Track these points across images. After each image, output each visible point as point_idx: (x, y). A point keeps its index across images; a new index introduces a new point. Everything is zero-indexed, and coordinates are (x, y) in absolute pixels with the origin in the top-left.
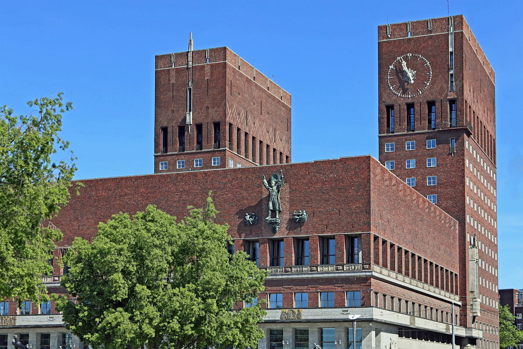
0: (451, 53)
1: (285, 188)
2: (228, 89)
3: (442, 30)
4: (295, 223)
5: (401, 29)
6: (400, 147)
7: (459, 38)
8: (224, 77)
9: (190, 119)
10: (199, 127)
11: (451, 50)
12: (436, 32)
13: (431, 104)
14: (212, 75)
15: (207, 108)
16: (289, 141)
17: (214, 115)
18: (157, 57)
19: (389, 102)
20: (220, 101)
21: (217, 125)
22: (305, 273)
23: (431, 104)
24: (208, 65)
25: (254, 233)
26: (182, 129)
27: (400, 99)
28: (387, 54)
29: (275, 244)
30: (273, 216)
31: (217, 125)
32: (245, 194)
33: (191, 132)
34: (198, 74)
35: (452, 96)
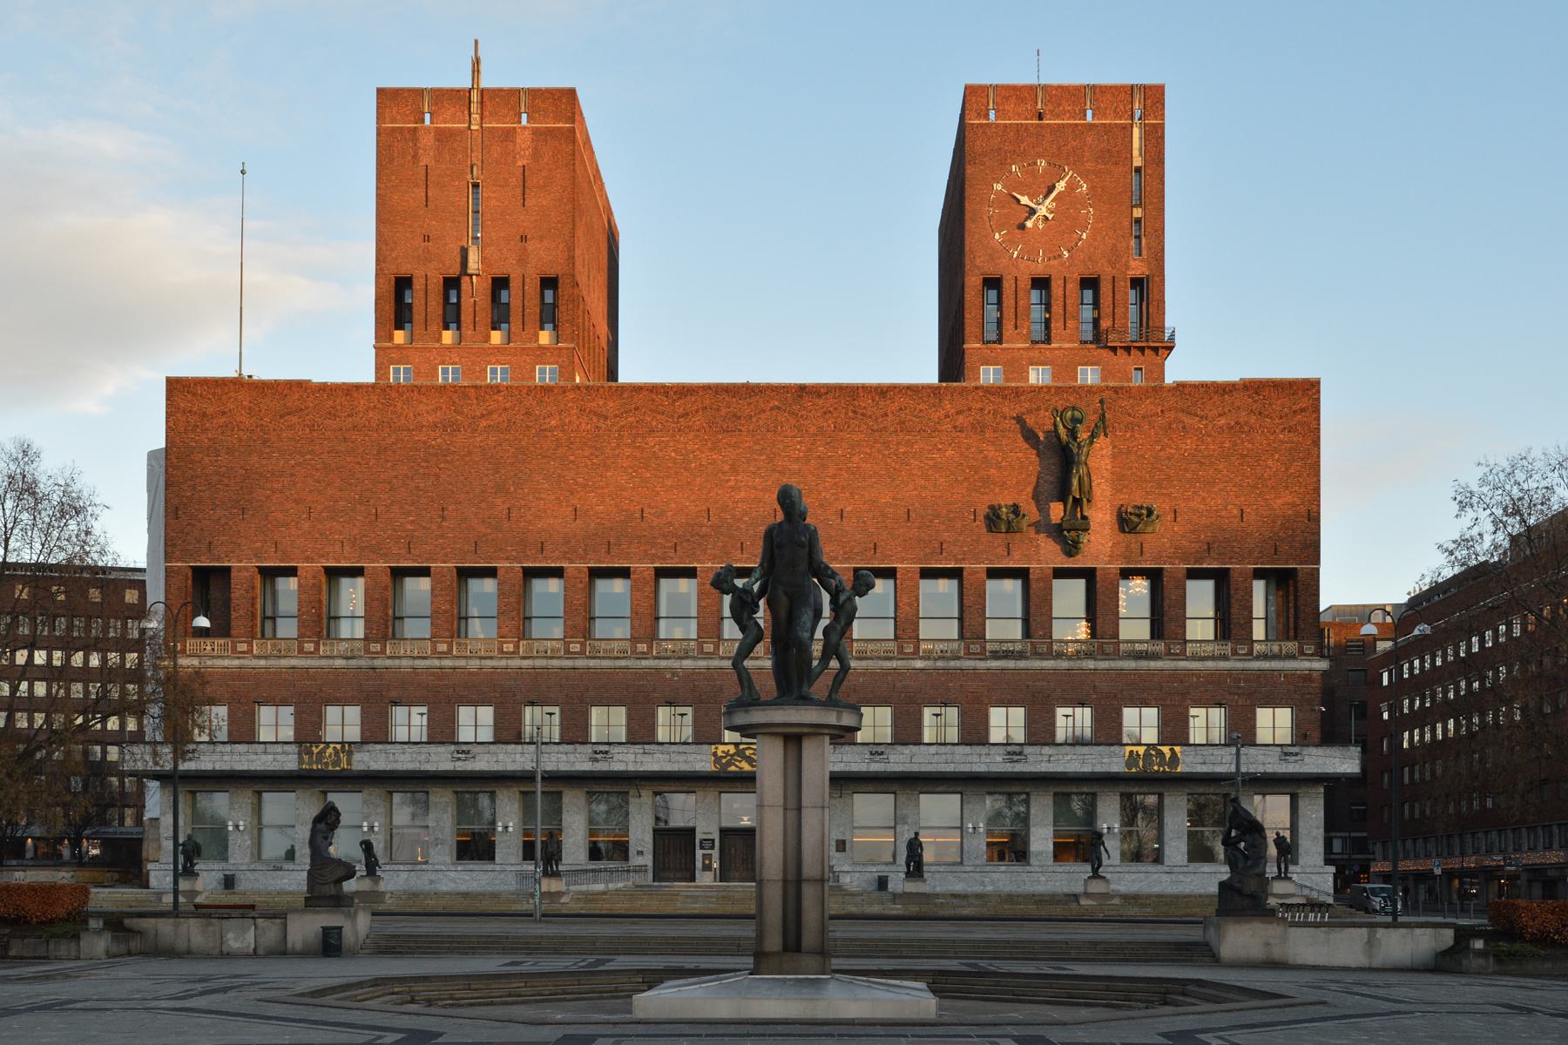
0: (1138, 170)
3: (1117, 115)
5: (1021, 100)
11: (1138, 162)
12: (1105, 116)
13: (1091, 283)
14: (536, 155)
15: (524, 238)
18: (380, 91)
24: (428, 129)
25: (1016, 554)
26: (452, 283)
32: (991, 452)
33: (475, 293)
34: (496, 150)
35: (1138, 268)
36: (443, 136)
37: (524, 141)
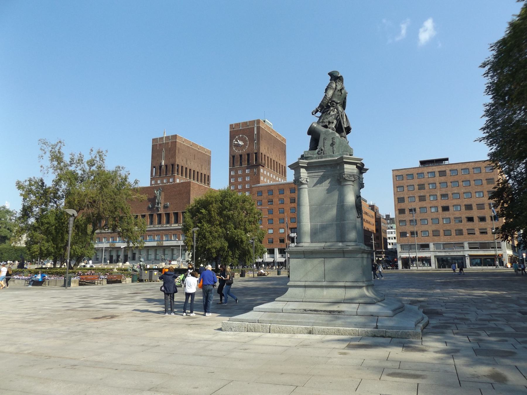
1: (163, 194)
2: (177, 151)
4: (165, 207)
6: (236, 172)
7: (259, 128)
8: (176, 146)
9: (163, 163)
10: (166, 166)
11: (255, 133)
16: (209, 169)
17: (171, 161)
19: (233, 155)
20: (174, 156)
21: (173, 165)
22: (168, 226)
23: (248, 155)
26: (161, 167)
27: (237, 152)
28: (232, 136)
29: (160, 215)
30: (158, 205)
31: (173, 165)
35: (255, 151)
36: (160, 145)
37: (170, 144)
